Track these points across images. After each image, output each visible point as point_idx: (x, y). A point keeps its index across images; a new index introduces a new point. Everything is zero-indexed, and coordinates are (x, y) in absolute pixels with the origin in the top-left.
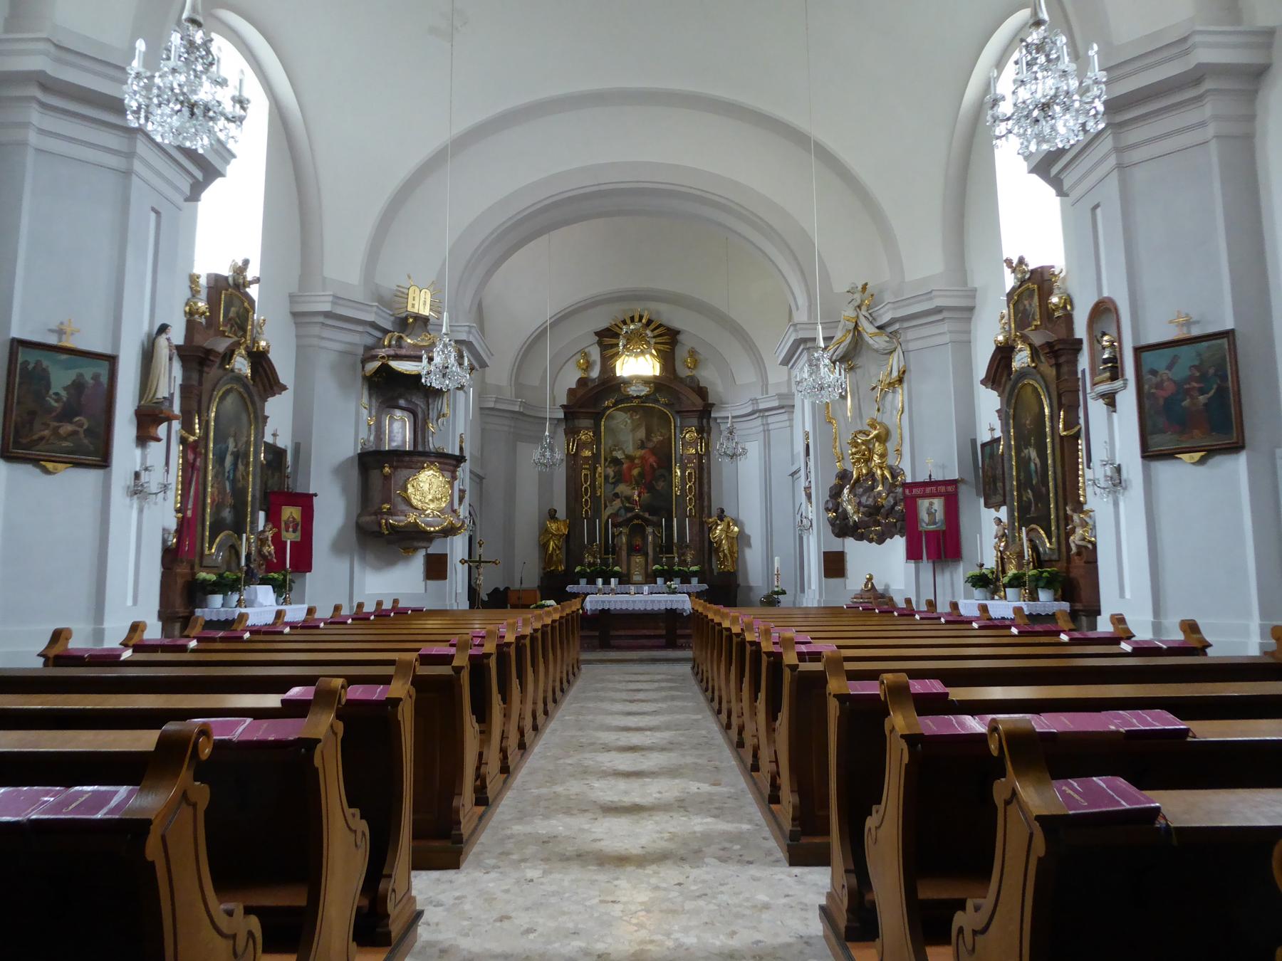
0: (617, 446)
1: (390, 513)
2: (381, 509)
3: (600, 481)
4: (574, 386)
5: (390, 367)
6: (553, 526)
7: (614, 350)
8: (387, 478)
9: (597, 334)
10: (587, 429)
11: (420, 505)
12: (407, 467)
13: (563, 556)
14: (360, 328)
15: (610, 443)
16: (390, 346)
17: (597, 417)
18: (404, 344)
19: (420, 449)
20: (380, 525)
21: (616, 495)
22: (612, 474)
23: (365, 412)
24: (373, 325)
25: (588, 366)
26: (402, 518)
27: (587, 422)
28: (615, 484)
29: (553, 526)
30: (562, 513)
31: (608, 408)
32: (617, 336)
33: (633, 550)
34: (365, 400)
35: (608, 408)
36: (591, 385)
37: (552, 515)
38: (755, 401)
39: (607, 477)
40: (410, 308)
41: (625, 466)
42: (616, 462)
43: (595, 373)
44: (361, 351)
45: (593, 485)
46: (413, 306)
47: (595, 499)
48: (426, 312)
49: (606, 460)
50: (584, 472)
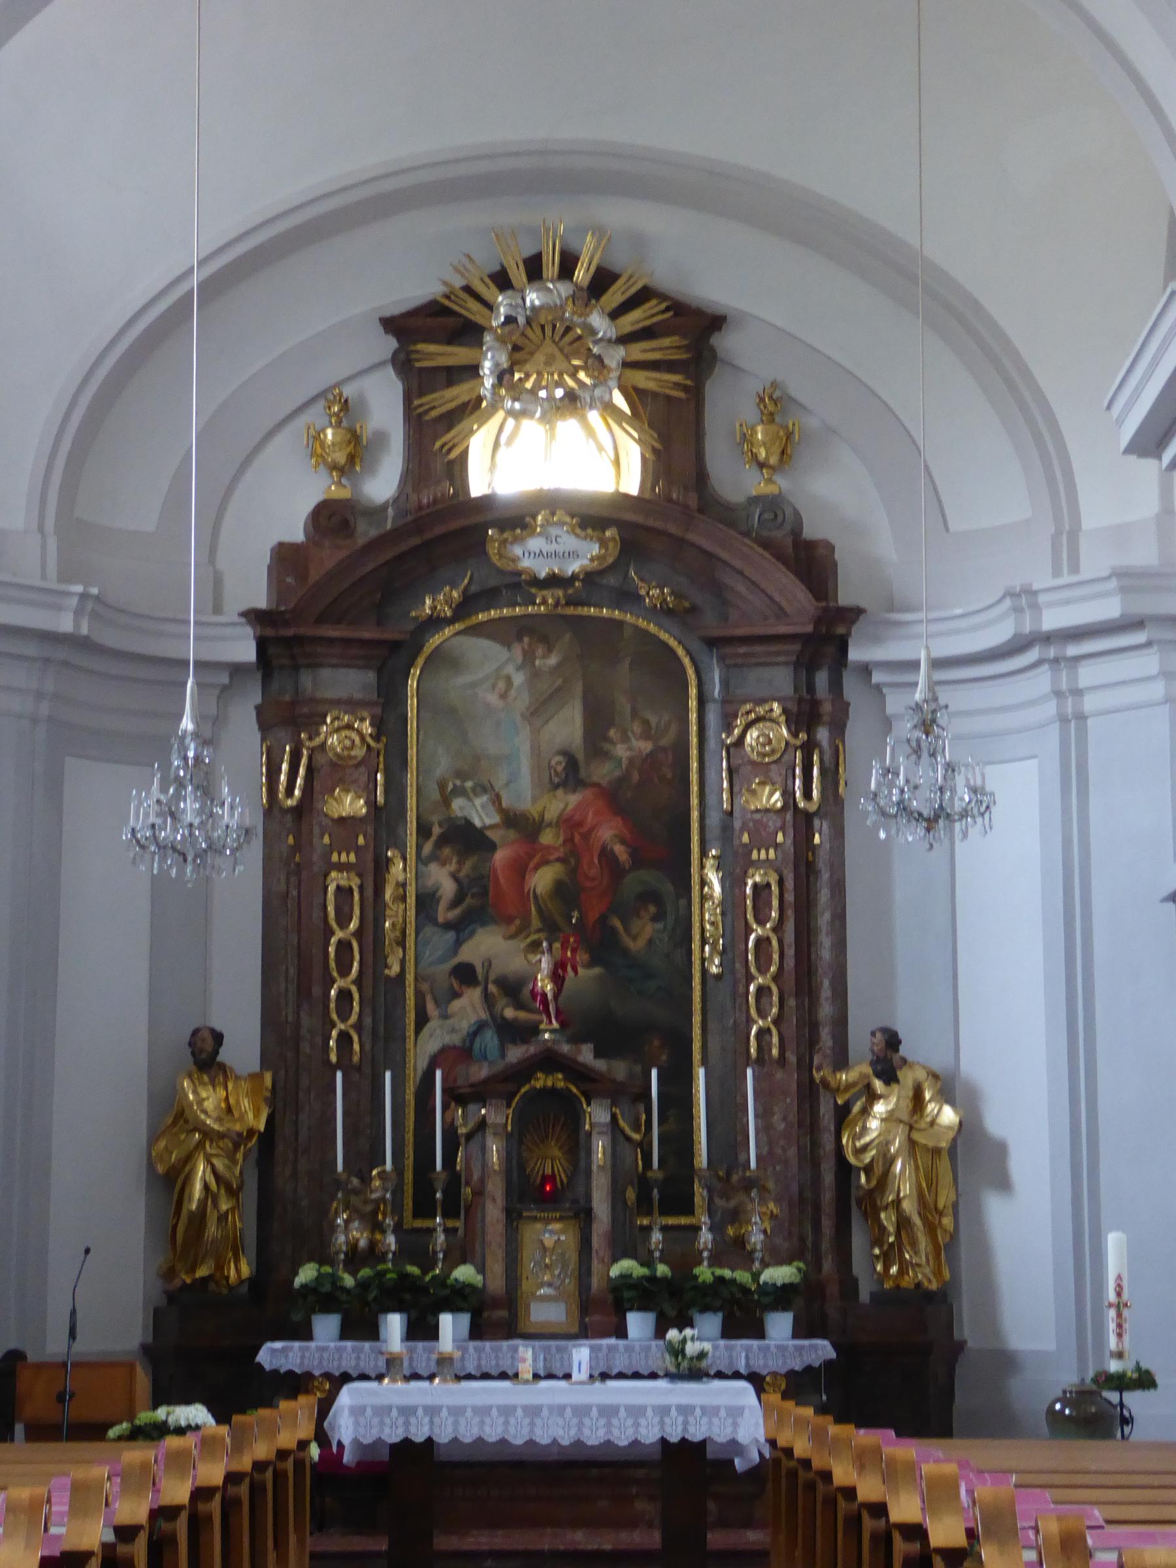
0: (472, 775)
3: (398, 915)
4: (298, 535)
6: (207, 1100)
7: (459, 393)
9: (391, 324)
10: (351, 705)
13: (245, 1223)
15: (443, 765)
17: (391, 659)
21: (466, 975)
22: (448, 888)
25: (357, 454)
27: (353, 681)
28: (461, 928)
29: (207, 1100)
30: (243, 1048)
31: (435, 622)
32: (469, 333)
33: (531, 1195)
35: (435, 622)
36: (366, 532)
37: (205, 1054)
38: (1024, 598)
39: (426, 902)
41: (500, 856)
42: (465, 839)
43: (382, 484)
47: (382, 991)
49: (424, 831)
50: (336, 879)
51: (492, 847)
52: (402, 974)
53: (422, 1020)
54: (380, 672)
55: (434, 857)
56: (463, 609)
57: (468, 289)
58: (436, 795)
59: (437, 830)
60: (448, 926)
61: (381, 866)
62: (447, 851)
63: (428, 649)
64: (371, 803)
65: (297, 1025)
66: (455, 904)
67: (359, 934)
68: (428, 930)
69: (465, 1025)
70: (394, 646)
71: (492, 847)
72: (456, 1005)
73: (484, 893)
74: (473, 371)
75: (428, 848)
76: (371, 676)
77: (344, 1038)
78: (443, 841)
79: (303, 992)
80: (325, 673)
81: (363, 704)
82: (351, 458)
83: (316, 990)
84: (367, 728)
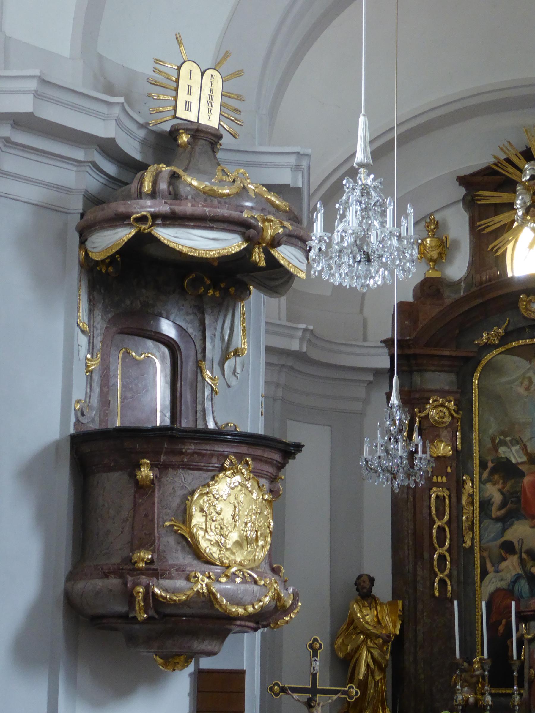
0: (510, 434)
1: (154, 571)
2: (129, 560)
3: (470, 512)
4: (410, 298)
5: (156, 241)
6: (366, 616)
7: (502, 218)
8: (144, 490)
9: (464, 181)
10: (443, 393)
11: (214, 552)
12: (188, 467)
13: (386, 687)
14: (79, 154)
15: (493, 428)
16: (154, 194)
17: (464, 367)
18: (183, 190)
19: (185, 423)
20: (131, 598)
21: (509, 548)
22: (497, 498)
23: (83, 340)
24: (108, 148)
25: (444, 251)
26: (181, 583)
27: (440, 380)
28: (506, 521)
29: (366, 616)
30: (383, 589)
31: (489, 347)
32: (509, 185)
34: (83, 315)
35: (489, 347)
36: (449, 297)
37: (364, 589)
39: (485, 505)
40: (181, 113)
41: (527, 480)
42: (506, 470)
43: (457, 269)
44: (77, 205)
45: (455, 521)
46: (188, 106)
47: (462, 555)
48: (211, 119)
49: (483, 465)
50: (435, 492)
51: (522, 475)
52: (472, 547)
53: (484, 573)
54: (458, 374)
55: (489, 480)
56: (504, 340)
57: (508, 160)
58: (490, 445)
59: (490, 465)
60: (498, 520)
61: (461, 484)
62: (496, 477)
63: (483, 363)
64: (455, 449)
65: (415, 574)
66: (501, 507)
67: (449, 523)
68: (487, 522)
69: (509, 577)
70: (466, 359)
71: (522, 475)
72: (503, 565)
73: (519, 501)
74: (511, 206)
75: (485, 475)
76: (453, 377)
77: (442, 582)
78: (494, 471)
79: (418, 555)
80: (428, 375)
81: (450, 392)
82: (440, 255)
83: (426, 555)
84: (452, 406)
